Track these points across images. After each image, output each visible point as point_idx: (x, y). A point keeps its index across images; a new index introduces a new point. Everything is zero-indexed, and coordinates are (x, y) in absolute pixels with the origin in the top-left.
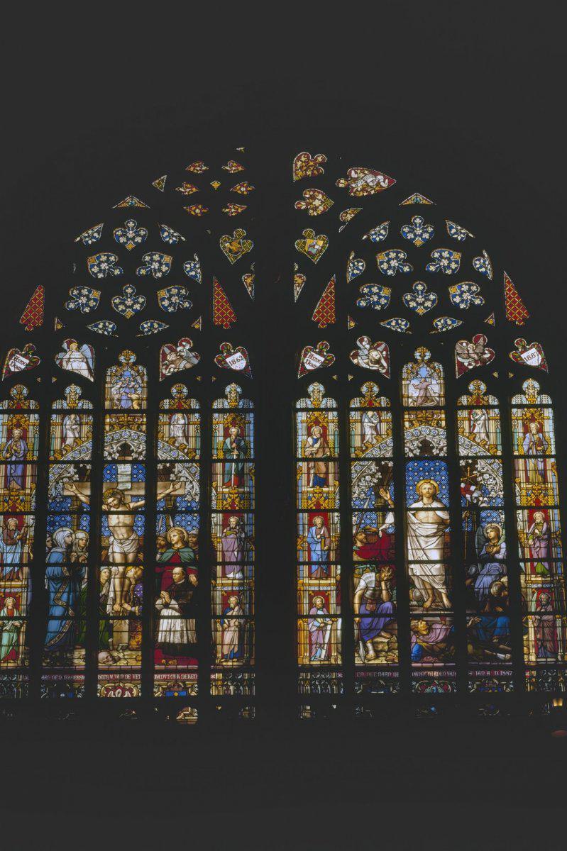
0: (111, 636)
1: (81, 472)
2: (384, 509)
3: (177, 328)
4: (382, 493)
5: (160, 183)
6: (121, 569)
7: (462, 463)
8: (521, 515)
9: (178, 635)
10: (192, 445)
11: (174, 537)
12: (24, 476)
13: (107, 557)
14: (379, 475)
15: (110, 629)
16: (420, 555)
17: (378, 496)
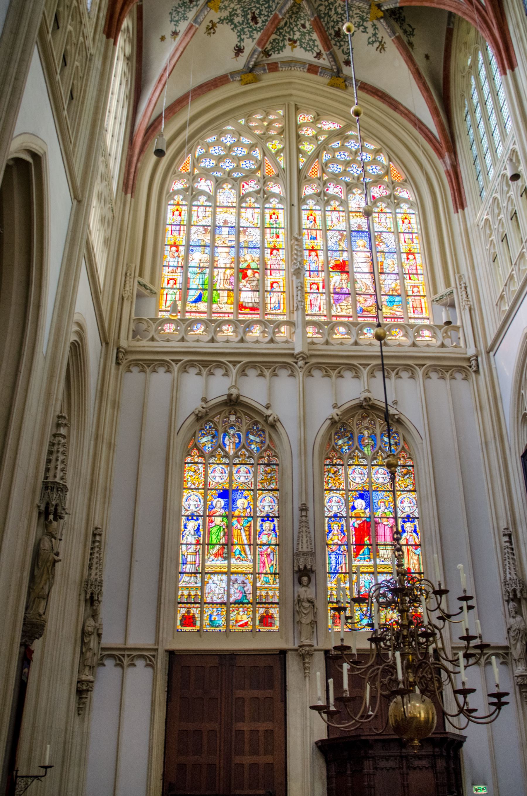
1: (206, 230)
4: (341, 244)
5: (242, 121)
6: (224, 270)
9: (250, 299)
10: (256, 221)
11: (248, 257)
12: (180, 230)
14: (340, 237)
15: (218, 296)
16: (359, 270)
17: (339, 245)
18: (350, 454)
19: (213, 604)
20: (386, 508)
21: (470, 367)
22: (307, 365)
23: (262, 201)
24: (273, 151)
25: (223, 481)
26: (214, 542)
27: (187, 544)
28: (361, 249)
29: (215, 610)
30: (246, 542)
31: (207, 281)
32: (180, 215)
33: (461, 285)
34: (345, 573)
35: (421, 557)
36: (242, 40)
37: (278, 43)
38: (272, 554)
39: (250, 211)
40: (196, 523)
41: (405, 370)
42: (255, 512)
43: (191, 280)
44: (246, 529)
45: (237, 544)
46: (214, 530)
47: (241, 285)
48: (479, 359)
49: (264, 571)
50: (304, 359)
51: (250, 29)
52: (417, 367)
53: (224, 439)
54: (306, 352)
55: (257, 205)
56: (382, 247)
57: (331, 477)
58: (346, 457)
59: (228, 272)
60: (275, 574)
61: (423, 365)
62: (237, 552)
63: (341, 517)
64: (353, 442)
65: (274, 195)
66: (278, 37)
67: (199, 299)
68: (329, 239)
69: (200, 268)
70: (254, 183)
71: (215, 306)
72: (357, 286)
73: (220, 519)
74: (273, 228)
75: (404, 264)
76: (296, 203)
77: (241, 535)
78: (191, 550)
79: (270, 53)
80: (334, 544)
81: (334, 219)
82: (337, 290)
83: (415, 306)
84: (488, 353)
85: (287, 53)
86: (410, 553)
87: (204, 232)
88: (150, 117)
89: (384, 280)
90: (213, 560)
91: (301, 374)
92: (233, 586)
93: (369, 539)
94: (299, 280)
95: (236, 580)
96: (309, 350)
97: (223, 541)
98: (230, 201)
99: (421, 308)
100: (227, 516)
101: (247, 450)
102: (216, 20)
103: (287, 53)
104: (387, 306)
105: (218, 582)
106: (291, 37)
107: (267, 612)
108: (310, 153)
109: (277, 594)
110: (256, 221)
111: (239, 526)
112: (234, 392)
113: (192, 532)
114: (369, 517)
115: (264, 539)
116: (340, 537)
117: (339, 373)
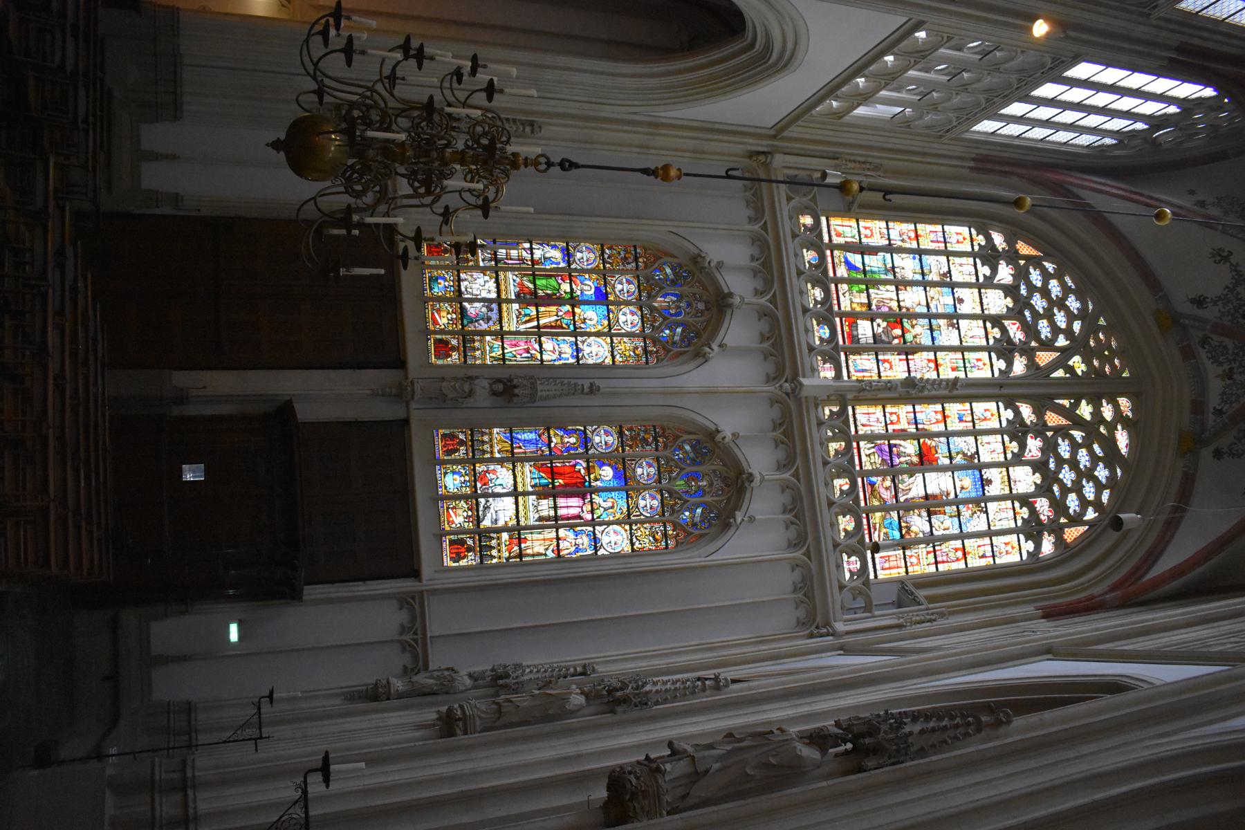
0: (857, 292)
1: (944, 275)
2: (951, 458)
3: (1030, 330)
4: (960, 456)
5: (1102, 322)
7: (983, 505)
8: (958, 544)
10: (969, 340)
11: (918, 330)
12: (938, 242)
13: (901, 290)
14: (969, 454)
15: (860, 291)
17: (958, 453)
18: (673, 460)
19: (459, 280)
20: (605, 510)
21: (817, 627)
22: (786, 397)
23: (998, 346)
24: (1071, 363)
25: (618, 293)
26: (538, 282)
27: (531, 249)
28: (958, 485)
29: (452, 283)
30: (542, 322)
31: (877, 276)
32: (958, 242)
33: (932, 614)
34: (513, 453)
35: (543, 557)
36: (1215, 303)
37: (1222, 355)
38: (529, 355)
39: (982, 332)
40: (559, 260)
41: (799, 535)
42: (583, 334)
43: (875, 257)
44: (559, 322)
45: (538, 311)
46: (552, 282)
47: (879, 321)
48: (830, 638)
49: (505, 346)
50: (793, 390)
51: (1232, 311)
52: (804, 549)
53: (672, 294)
54: (804, 393)
55: (991, 342)
56: (966, 512)
57: (639, 434)
58: (667, 453)
59: (894, 305)
60: (504, 359)
61: (809, 558)
62: (527, 311)
63: (586, 447)
64: (689, 465)
65: (1010, 364)
66: (1230, 352)
67: (850, 267)
68: (964, 439)
69: (893, 267)
70: (1021, 337)
71: (845, 287)
72: (905, 477)
73: (568, 290)
74: (964, 363)
75: (947, 544)
76: (1005, 391)
77: (550, 316)
78: (524, 254)
79: (1206, 346)
80: (549, 437)
81: (992, 447)
82: (894, 449)
83: (891, 559)
84: (841, 648)
85: (1213, 371)
86: (548, 543)
87: (942, 272)
88: (1083, 187)
89: (919, 515)
90: (514, 281)
91: (772, 388)
92: (483, 306)
93: (561, 485)
94: (899, 385)
95: (491, 310)
96: (806, 398)
97: (540, 293)
98: (990, 306)
99: (890, 568)
100: (572, 298)
101: (661, 324)
102: (1234, 260)
103: (1213, 371)
104: (884, 518)
105: (486, 287)
106: (1235, 371)
107: (454, 349)
108: (1077, 412)
109: (478, 362)
110: (969, 340)
111: (560, 314)
112: (736, 301)
113: (548, 255)
114: (590, 486)
115: (548, 344)
116: (559, 446)
117: (782, 443)
